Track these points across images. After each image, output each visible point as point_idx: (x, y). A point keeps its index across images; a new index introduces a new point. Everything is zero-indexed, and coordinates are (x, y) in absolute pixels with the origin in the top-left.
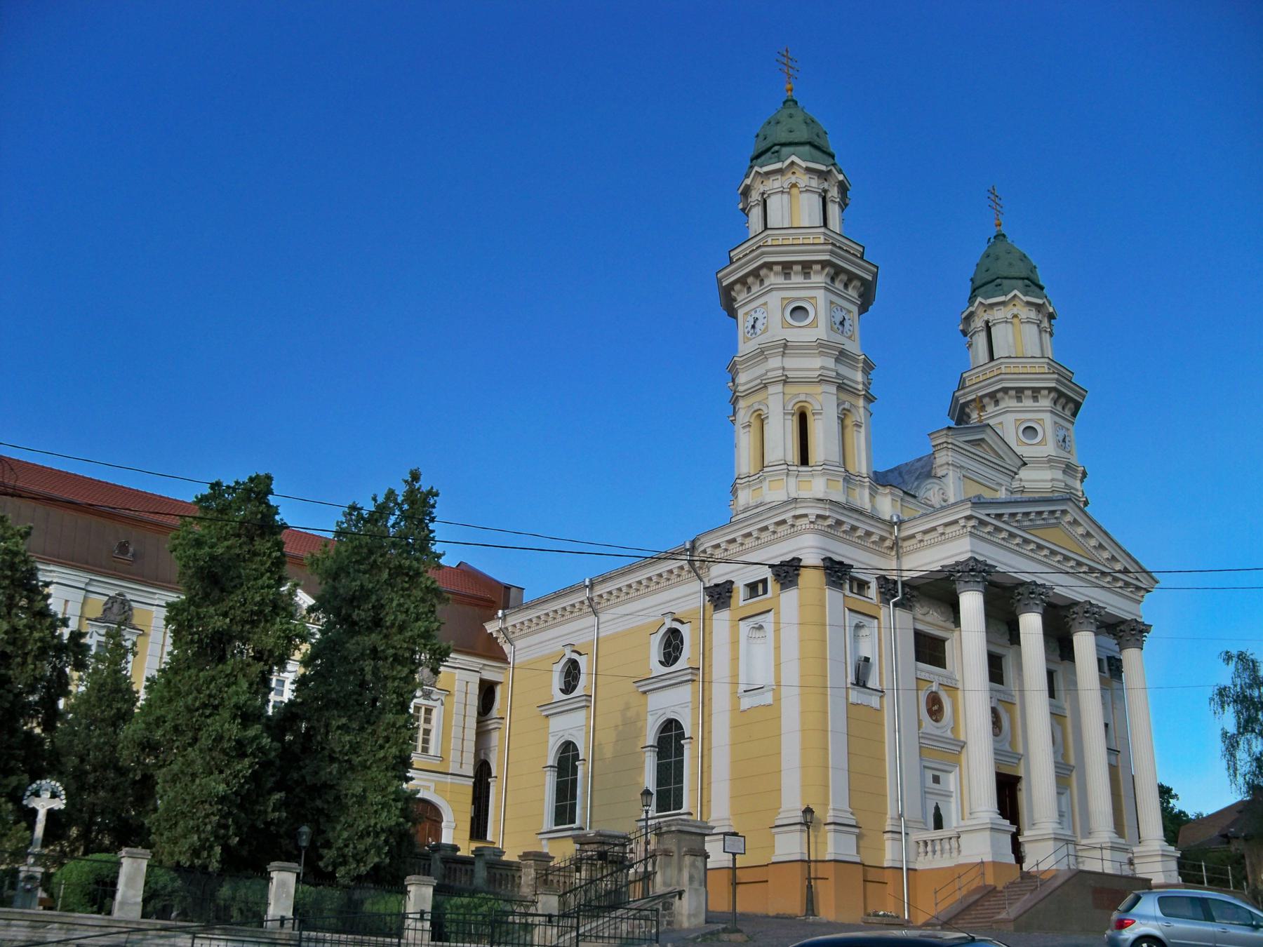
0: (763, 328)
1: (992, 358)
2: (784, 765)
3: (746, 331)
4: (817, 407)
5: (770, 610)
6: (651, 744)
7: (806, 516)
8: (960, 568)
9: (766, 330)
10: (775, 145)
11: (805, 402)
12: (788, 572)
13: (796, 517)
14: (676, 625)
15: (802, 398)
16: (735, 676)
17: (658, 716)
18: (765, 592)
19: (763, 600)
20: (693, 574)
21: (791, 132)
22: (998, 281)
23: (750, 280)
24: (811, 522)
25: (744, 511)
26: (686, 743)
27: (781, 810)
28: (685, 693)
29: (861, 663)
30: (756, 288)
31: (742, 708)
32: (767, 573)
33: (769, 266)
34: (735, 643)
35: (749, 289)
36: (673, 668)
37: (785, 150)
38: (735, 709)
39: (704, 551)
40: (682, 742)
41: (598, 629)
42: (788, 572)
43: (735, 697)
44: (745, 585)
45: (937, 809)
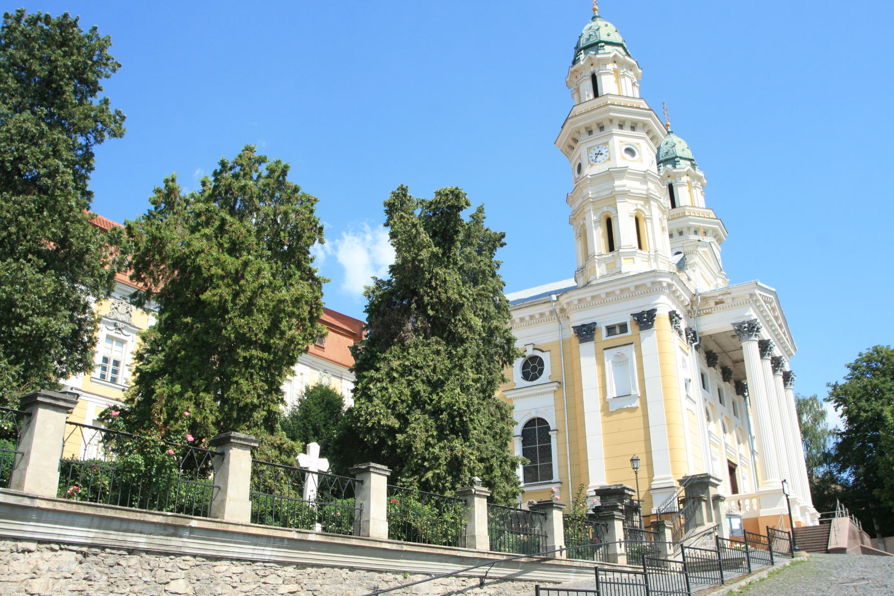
3: (590, 159)
4: (647, 214)
5: (632, 343)
7: (661, 282)
8: (746, 325)
10: (601, 42)
11: (640, 210)
13: (653, 283)
15: (639, 207)
18: (626, 331)
19: (621, 337)
21: (608, 35)
22: (678, 159)
23: (594, 128)
25: (602, 277)
30: (596, 132)
31: (611, 410)
32: (628, 319)
35: (590, 132)
37: (608, 48)
42: (645, 320)
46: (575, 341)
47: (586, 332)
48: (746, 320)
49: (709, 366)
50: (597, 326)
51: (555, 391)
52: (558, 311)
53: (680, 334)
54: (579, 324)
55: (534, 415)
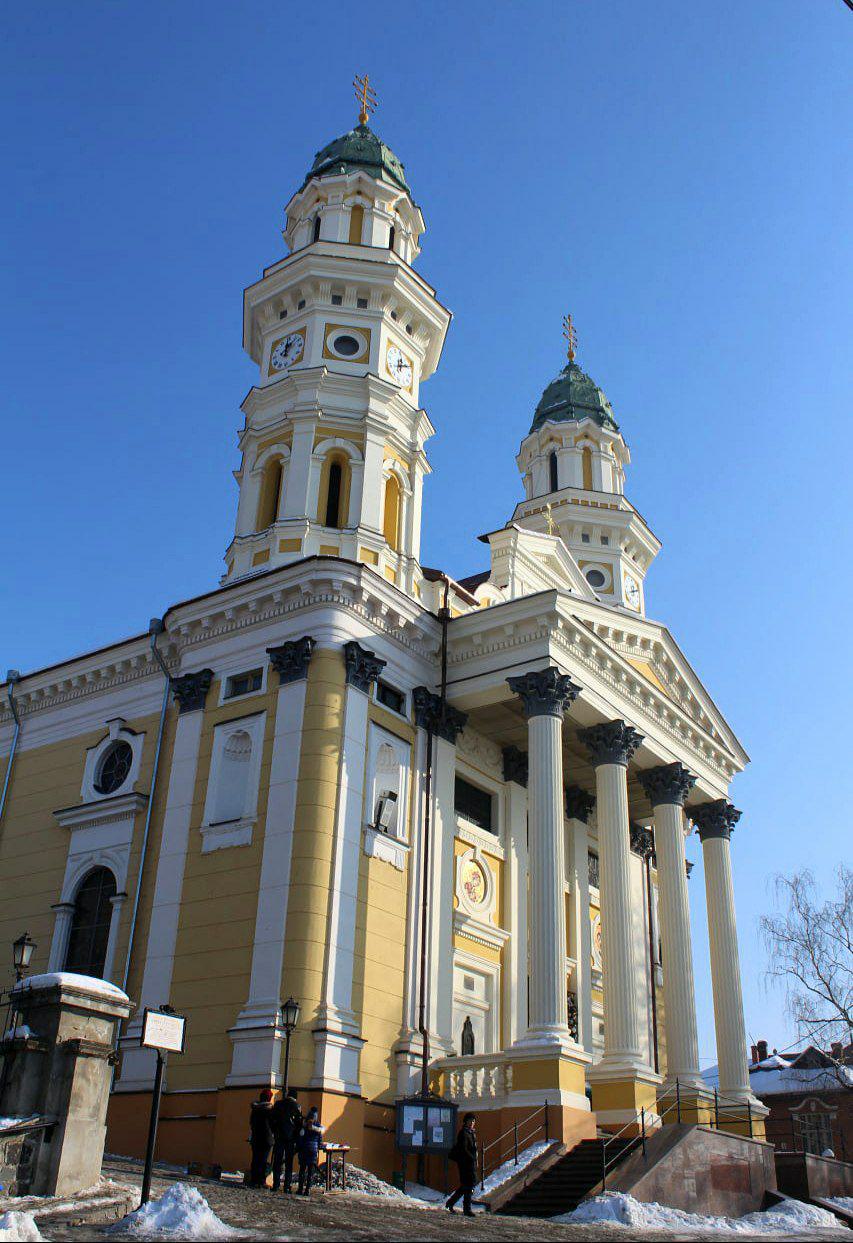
0: (296, 357)
1: (554, 487)
2: (260, 935)
5: (261, 712)
6: (68, 901)
7: (329, 582)
8: (533, 682)
9: (300, 359)
12: (294, 659)
13: (315, 583)
14: (126, 737)
15: (340, 443)
16: (199, 804)
17: (82, 861)
20: (157, 666)
23: (287, 301)
24: (337, 592)
26: (116, 901)
27: (248, 1004)
28: (124, 831)
29: (384, 800)
30: (292, 311)
31: (204, 849)
32: (264, 662)
33: (315, 282)
34: (204, 758)
35: (284, 314)
36: (113, 795)
38: (196, 854)
39: (178, 631)
40: (111, 899)
41: (18, 741)
42: (294, 659)
43: (196, 832)
44: (230, 679)
45: (468, 1025)
46: (175, 705)
47: (192, 691)
48: (536, 668)
49: (506, 781)
50: (216, 678)
51: (137, 813)
52: (165, 653)
53: (390, 696)
54: (182, 675)
55: (98, 861)
